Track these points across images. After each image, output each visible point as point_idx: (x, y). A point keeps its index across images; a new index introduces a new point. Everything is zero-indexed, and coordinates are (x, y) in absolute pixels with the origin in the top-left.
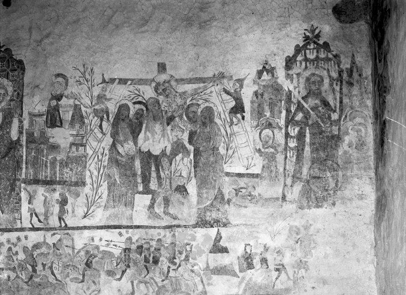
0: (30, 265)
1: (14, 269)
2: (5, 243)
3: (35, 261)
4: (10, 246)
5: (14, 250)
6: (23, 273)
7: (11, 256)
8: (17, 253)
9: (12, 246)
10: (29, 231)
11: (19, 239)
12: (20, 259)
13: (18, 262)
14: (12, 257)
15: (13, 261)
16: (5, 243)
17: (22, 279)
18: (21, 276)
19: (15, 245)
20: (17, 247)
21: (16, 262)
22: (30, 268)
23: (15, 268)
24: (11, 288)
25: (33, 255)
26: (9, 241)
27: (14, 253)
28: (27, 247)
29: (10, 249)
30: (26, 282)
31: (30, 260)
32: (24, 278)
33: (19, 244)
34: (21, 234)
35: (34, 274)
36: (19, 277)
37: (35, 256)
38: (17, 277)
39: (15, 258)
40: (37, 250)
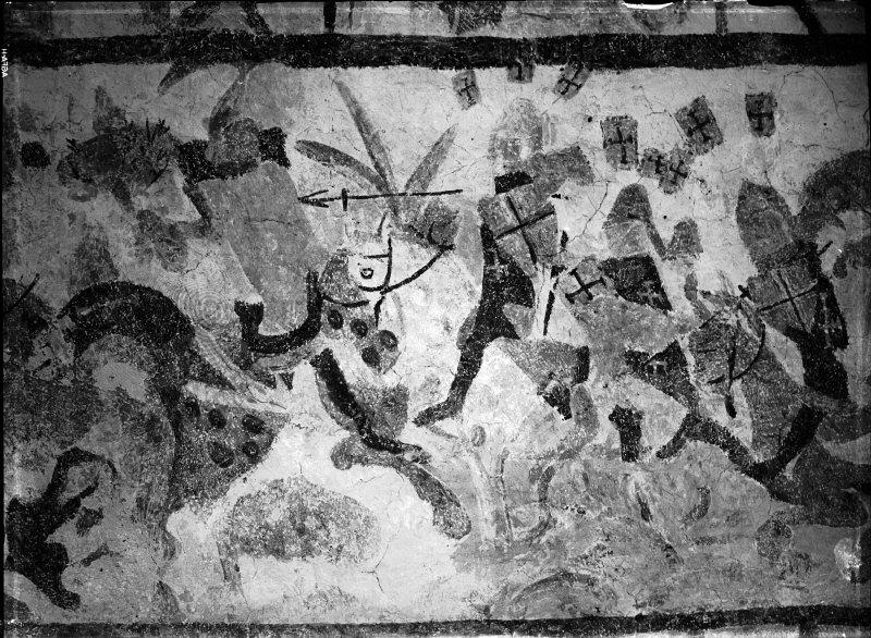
0: (790, 332)
1: (666, 369)
2: (600, 165)
3: (832, 302)
4: (630, 177)
5: (666, 208)
6: (741, 402)
7: (647, 261)
8: (687, 236)
9: (652, 186)
10: (784, 60)
11: (699, 124)
12: (714, 286)
13: (700, 310)
14: (652, 273)
15: (665, 305)
16: (600, 165)
17: (731, 444)
18: (721, 417)
19: (671, 172)
20: (690, 188)
21: (683, 308)
22: (793, 366)
23: (673, 354)
24: (645, 514)
25: (807, 254)
26: (621, 140)
27: (666, 234)
28: (768, 192)
29: (631, 206)
30: (758, 472)
31: (793, 288)
32: (744, 433)
33: (702, 165)
34: (723, 88)
35: (827, 404)
36: (709, 432)
37: (827, 265)
38: (696, 427)
39: (671, 278)
40: (845, 216)
